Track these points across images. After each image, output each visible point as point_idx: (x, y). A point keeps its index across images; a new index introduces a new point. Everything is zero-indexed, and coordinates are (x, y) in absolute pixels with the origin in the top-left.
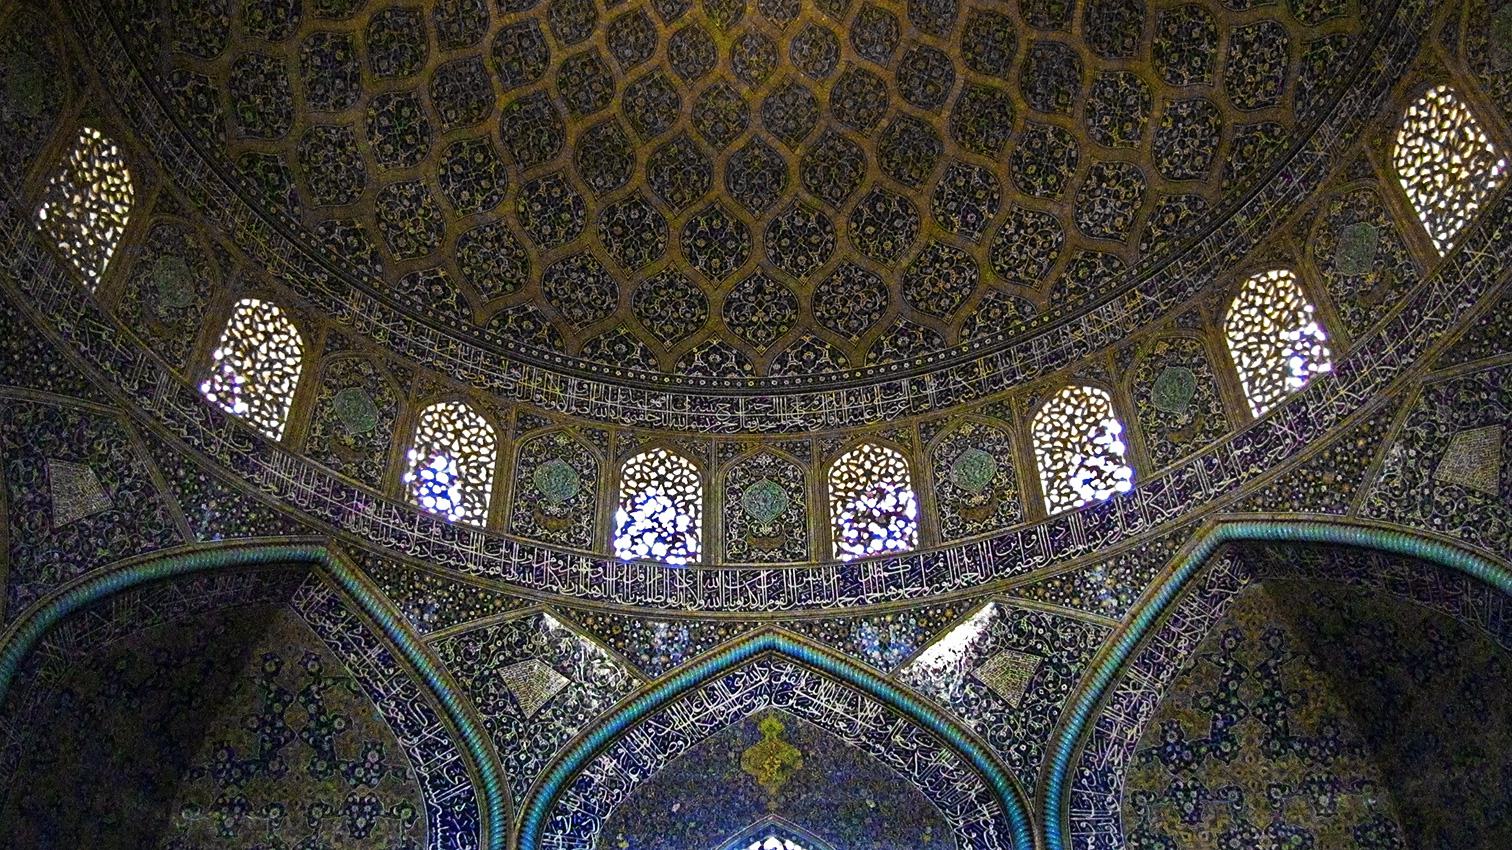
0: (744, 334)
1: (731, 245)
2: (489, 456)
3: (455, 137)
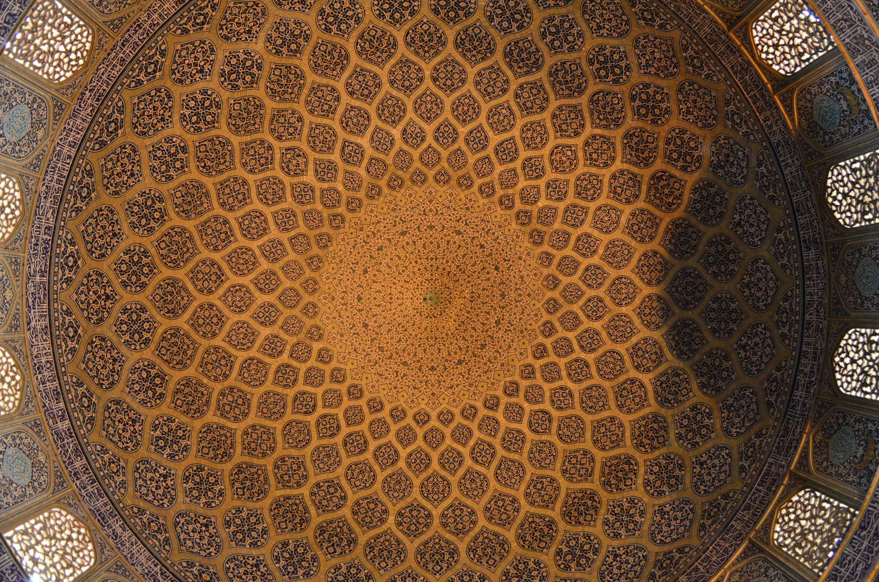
0: (83, 284)
1: (134, 278)
2: (47, 73)
3: (225, 106)
